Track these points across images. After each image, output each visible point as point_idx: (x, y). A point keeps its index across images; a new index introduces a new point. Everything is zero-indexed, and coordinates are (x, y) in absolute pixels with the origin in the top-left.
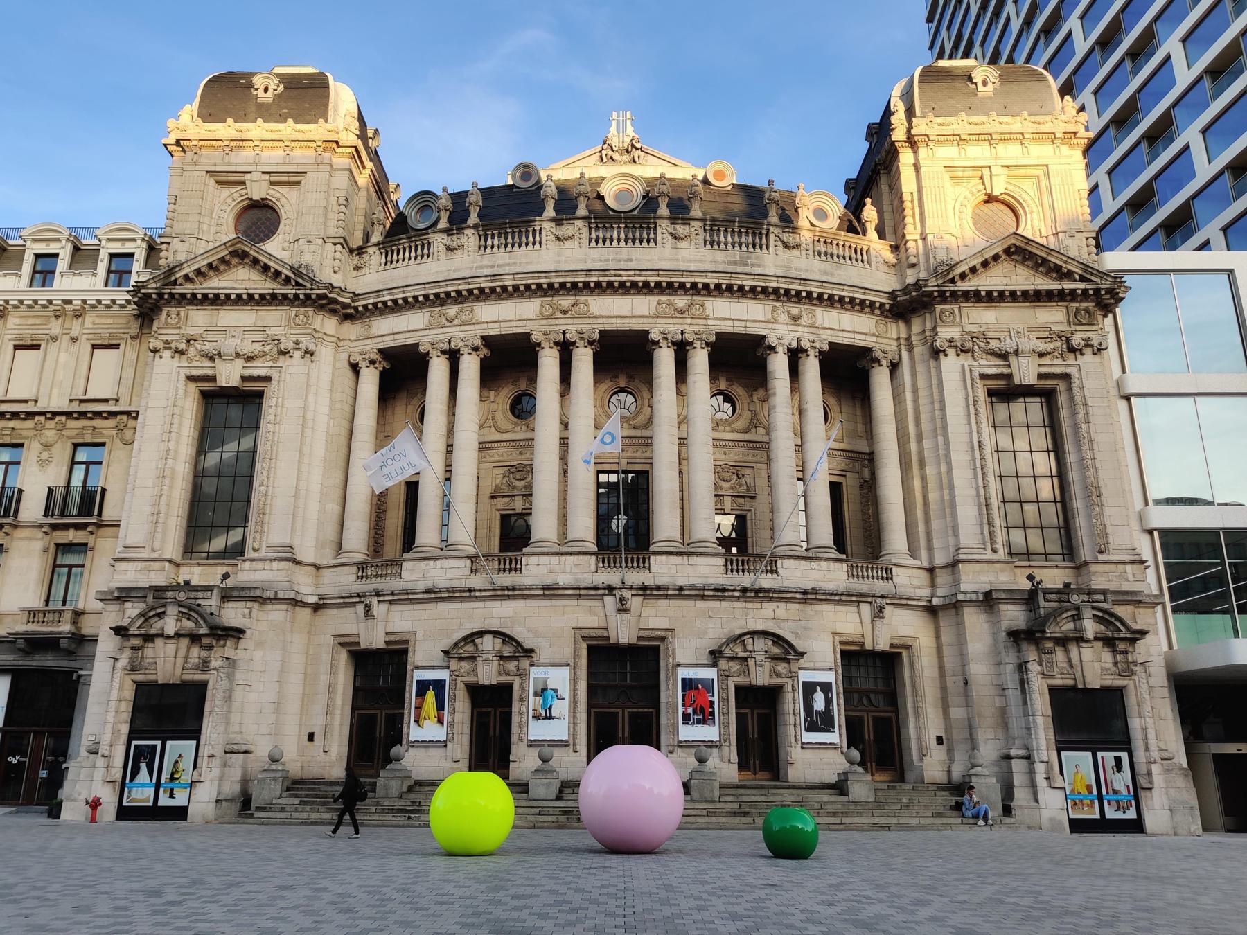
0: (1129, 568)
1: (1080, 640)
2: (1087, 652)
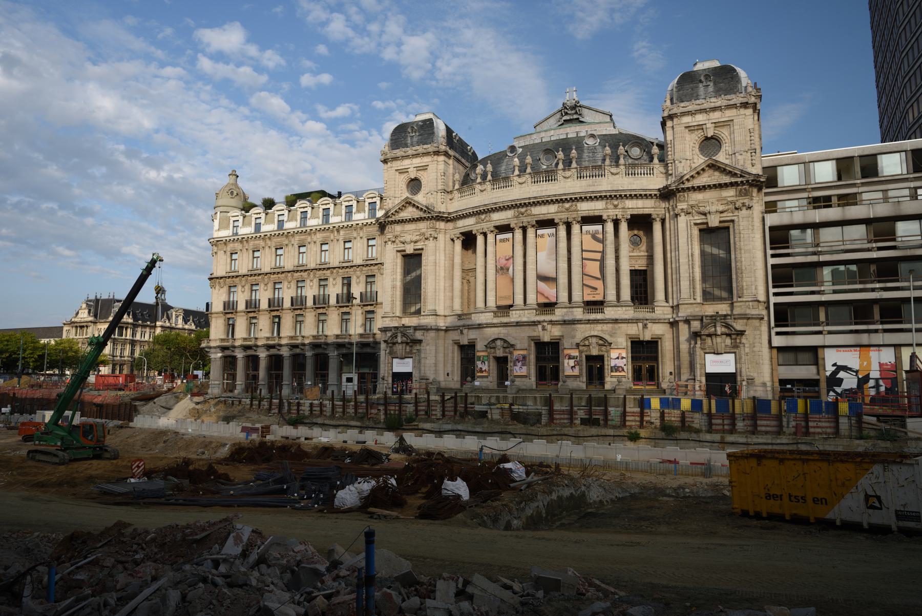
1: (716, 335)
2: (719, 340)
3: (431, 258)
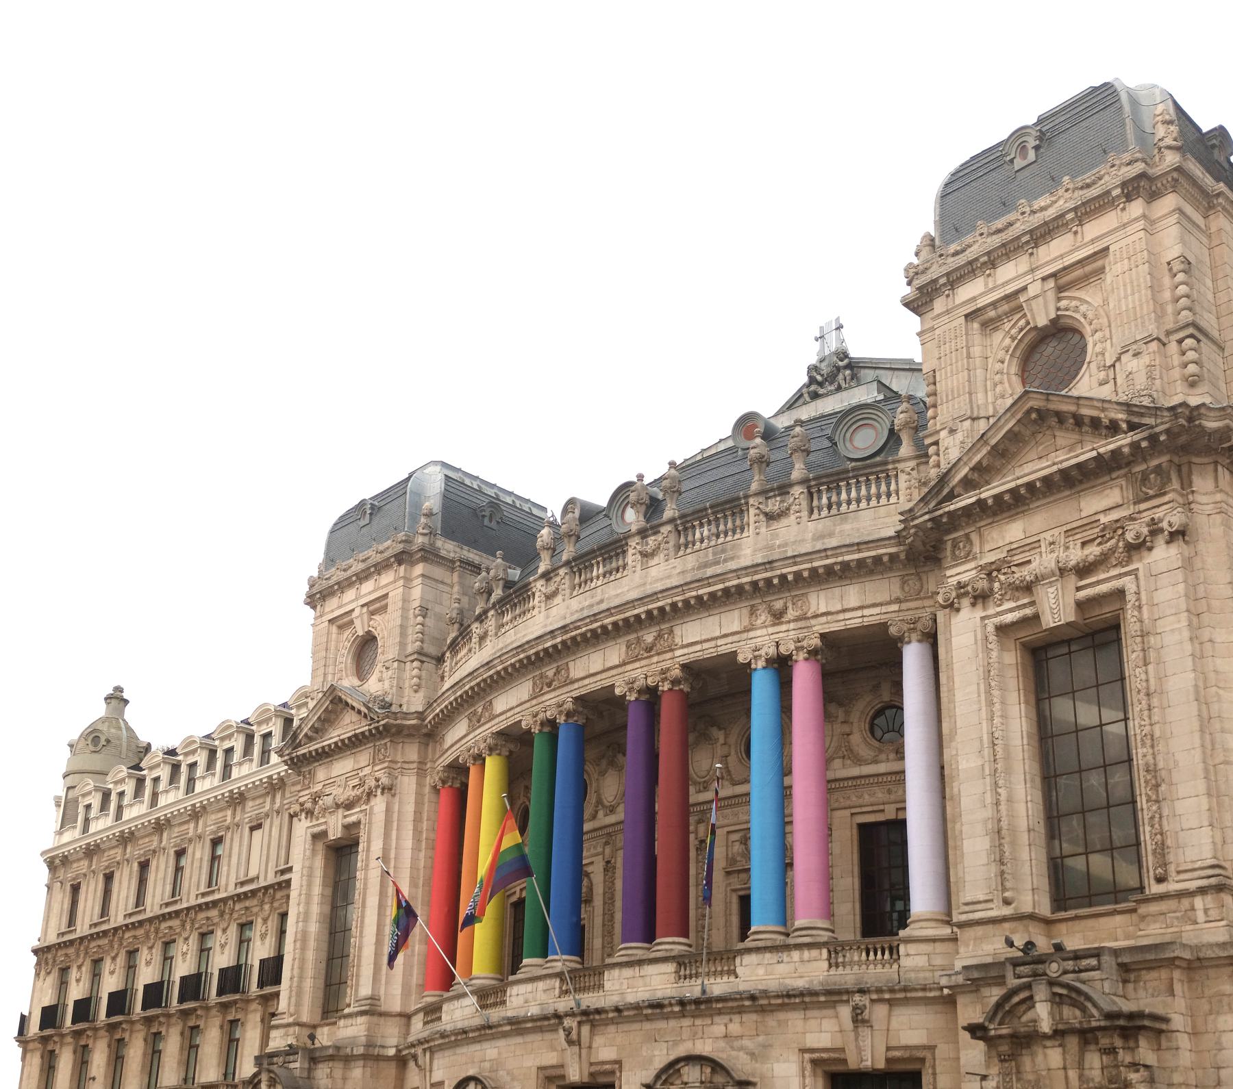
0: (1199, 902)
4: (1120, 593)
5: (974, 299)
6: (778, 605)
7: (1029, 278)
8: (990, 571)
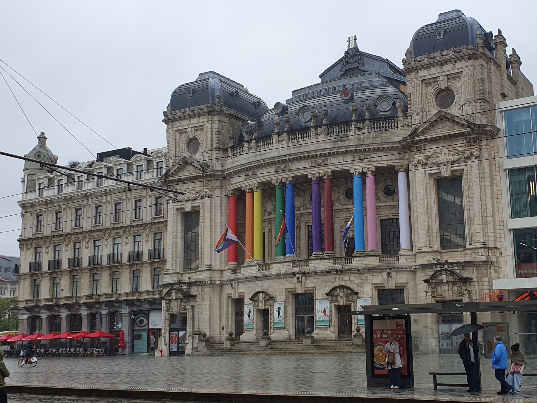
0: (479, 250)
3: (207, 215)
4: (463, 170)
5: (424, 76)
6: (362, 157)
7: (440, 74)
8: (427, 158)
